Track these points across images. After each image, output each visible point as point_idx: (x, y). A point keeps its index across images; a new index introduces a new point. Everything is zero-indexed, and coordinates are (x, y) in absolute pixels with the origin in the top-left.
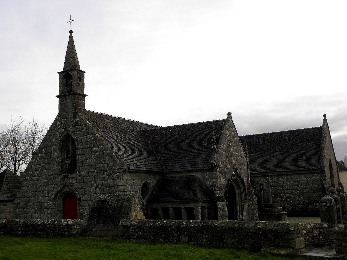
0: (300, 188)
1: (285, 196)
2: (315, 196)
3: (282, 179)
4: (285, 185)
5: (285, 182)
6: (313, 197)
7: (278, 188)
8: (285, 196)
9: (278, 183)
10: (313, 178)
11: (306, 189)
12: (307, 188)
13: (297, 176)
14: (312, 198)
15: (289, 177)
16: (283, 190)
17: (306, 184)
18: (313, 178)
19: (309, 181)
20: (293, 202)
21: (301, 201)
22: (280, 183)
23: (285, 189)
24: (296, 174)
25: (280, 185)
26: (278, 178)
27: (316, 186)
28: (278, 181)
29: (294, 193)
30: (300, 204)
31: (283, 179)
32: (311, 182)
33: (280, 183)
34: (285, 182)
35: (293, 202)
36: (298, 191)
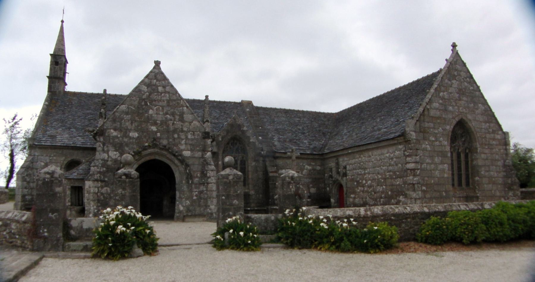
0: (382, 171)
1: (366, 185)
2: (399, 185)
3: (364, 158)
4: (367, 167)
5: (367, 162)
6: (397, 185)
7: (360, 171)
8: (366, 185)
9: (360, 165)
10: (397, 153)
11: (388, 172)
12: (390, 171)
13: (379, 152)
14: (395, 187)
15: (370, 153)
16: (365, 174)
17: (388, 164)
18: (397, 153)
19: (392, 159)
20: (375, 193)
21: (382, 192)
22: (362, 164)
23: (367, 173)
24: (377, 148)
25: (362, 167)
26: (360, 157)
27: (400, 167)
28: (360, 160)
29: (375, 179)
30: (381, 198)
31: (364, 158)
32: (395, 159)
33: (362, 164)
34: (367, 162)
35: (375, 193)
36: (380, 177)
